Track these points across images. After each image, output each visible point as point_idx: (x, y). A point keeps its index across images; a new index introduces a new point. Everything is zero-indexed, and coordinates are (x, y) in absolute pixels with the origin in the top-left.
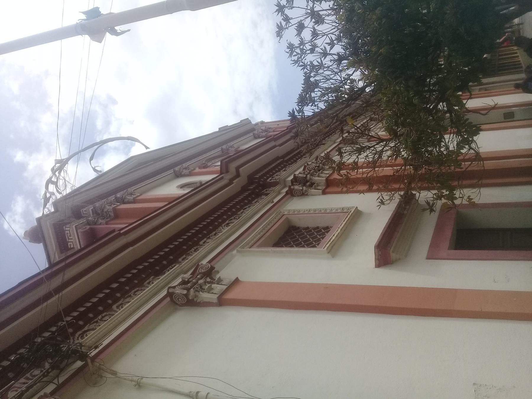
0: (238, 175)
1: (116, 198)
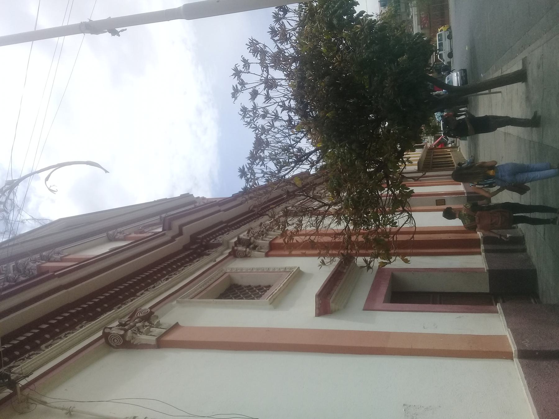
0: (180, 233)
1: (41, 256)
